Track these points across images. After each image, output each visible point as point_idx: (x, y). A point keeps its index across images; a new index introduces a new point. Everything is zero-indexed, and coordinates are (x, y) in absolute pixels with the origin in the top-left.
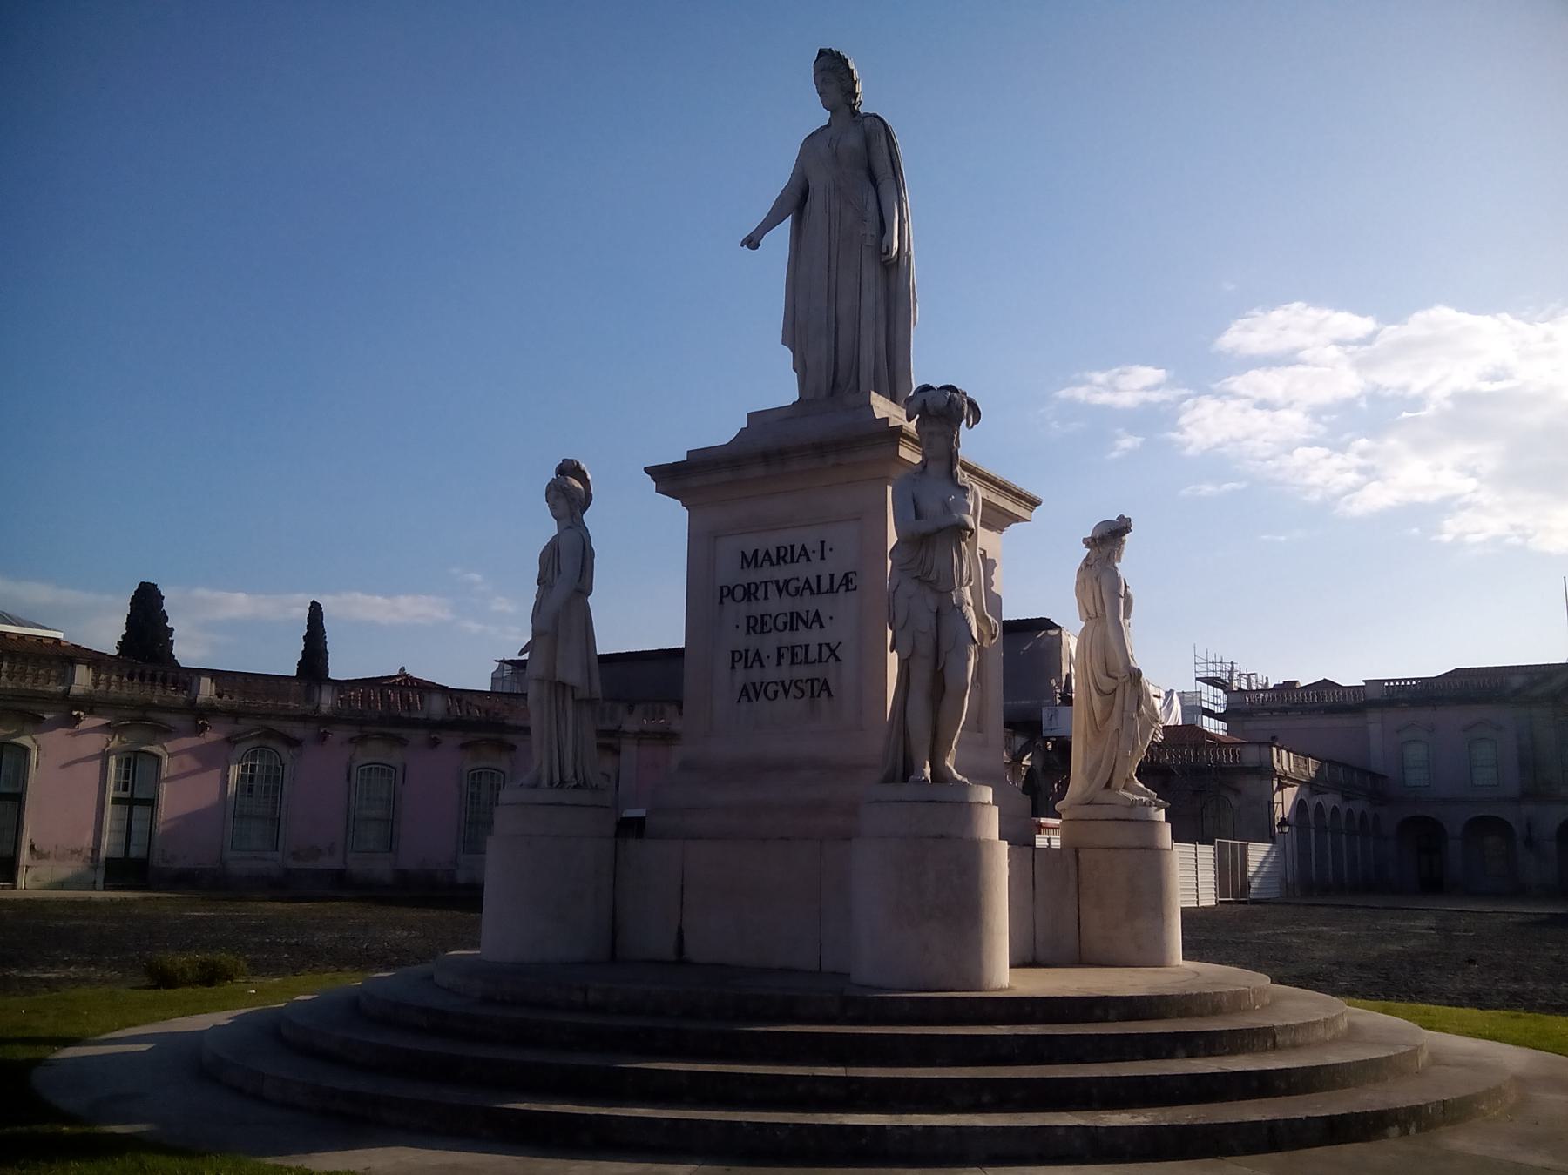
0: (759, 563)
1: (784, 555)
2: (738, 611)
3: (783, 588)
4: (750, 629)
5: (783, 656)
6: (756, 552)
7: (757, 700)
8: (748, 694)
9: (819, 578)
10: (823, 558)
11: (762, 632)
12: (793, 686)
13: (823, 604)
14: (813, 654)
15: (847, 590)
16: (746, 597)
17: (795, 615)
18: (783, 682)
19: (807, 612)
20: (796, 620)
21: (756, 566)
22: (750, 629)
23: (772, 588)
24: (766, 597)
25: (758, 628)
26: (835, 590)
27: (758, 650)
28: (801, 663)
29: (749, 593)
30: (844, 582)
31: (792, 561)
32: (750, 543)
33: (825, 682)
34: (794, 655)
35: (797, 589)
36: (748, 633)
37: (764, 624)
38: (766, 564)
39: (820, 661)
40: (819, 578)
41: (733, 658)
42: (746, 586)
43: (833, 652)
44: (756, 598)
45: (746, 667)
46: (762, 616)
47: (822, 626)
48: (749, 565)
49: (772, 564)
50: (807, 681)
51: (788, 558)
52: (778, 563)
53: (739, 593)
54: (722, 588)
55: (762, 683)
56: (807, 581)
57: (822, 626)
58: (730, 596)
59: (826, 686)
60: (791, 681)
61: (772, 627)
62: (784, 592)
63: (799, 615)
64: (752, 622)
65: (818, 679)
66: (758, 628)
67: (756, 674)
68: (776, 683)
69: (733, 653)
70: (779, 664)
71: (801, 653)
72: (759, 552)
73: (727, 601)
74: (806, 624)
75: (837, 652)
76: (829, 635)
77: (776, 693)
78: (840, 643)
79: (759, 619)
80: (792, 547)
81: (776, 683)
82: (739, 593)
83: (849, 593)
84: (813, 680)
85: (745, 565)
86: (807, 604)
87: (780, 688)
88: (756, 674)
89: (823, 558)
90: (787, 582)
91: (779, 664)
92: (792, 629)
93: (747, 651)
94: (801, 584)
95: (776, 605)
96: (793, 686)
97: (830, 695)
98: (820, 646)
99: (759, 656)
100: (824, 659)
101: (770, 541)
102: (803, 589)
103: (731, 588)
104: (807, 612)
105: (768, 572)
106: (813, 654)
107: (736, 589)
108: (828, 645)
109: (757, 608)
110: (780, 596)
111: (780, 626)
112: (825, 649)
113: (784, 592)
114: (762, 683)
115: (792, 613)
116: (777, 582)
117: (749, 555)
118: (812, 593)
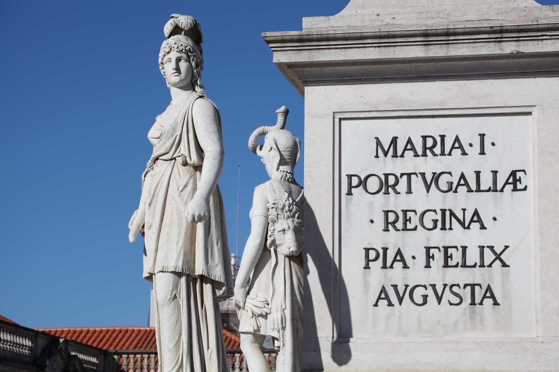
0: (399, 153)
4: (388, 225)
5: (433, 257)
6: (394, 141)
7: (400, 304)
8: (387, 298)
9: (478, 173)
11: (405, 229)
14: (473, 257)
15: (515, 189)
17: (448, 213)
18: (433, 286)
19: (464, 210)
21: (395, 156)
23: (417, 182)
24: (409, 192)
25: (399, 225)
26: (499, 188)
27: (399, 249)
28: (456, 266)
30: (511, 180)
31: (443, 154)
33: (489, 289)
34: (447, 257)
37: (407, 220)
38: (409, 154)
39: (482, 266)
40: (478, 173)
41: (367, 255)
42: (383, 178)
43: (498, 257)
45: (384, 267)
46: (405, 212)
47: (483, 227)
48: (386, 154)
49: (416, 155)
50: (465, 286)
51: (437, 150)
52: (424, 155)
53: (373, 185)
55: (407, 286)
56: (462, 176)
57: (483, 227)
59: (489, 293)
60: (445, 285)
63: (452, 214)
65: (479, 285)
66: (399, 225)
68: (425, 287)
69: (367, 250)
70: (428, 266)
71: (457, 257)
73: (358, 192)
74: (462, 224)
75: (502, 257)
77: (425, 297)
78: (507, 247)
79: (401, 214)
80: (443, 137)
81: (425, 287)
82: (373, 185)
84: (473, 286)
85: (381, 153)
87: (430, 292)
89: (482, 153)
90: (436, 177)
91: (428, 266)
92: (443, 228)
93: (385, 250)
94: (455, 180)
96: (447, 288)
97: (496, 303)
98: (482, 248)
99: (402, 256)
100: (487, 263)
102: (459, 184)
104: (464, 210)
106: (473, 257)
107: (369, 181)
110: (428, 191)
112: (487, 251)
114: (407, 286)
115: (443, 211)
116: (423, 175)
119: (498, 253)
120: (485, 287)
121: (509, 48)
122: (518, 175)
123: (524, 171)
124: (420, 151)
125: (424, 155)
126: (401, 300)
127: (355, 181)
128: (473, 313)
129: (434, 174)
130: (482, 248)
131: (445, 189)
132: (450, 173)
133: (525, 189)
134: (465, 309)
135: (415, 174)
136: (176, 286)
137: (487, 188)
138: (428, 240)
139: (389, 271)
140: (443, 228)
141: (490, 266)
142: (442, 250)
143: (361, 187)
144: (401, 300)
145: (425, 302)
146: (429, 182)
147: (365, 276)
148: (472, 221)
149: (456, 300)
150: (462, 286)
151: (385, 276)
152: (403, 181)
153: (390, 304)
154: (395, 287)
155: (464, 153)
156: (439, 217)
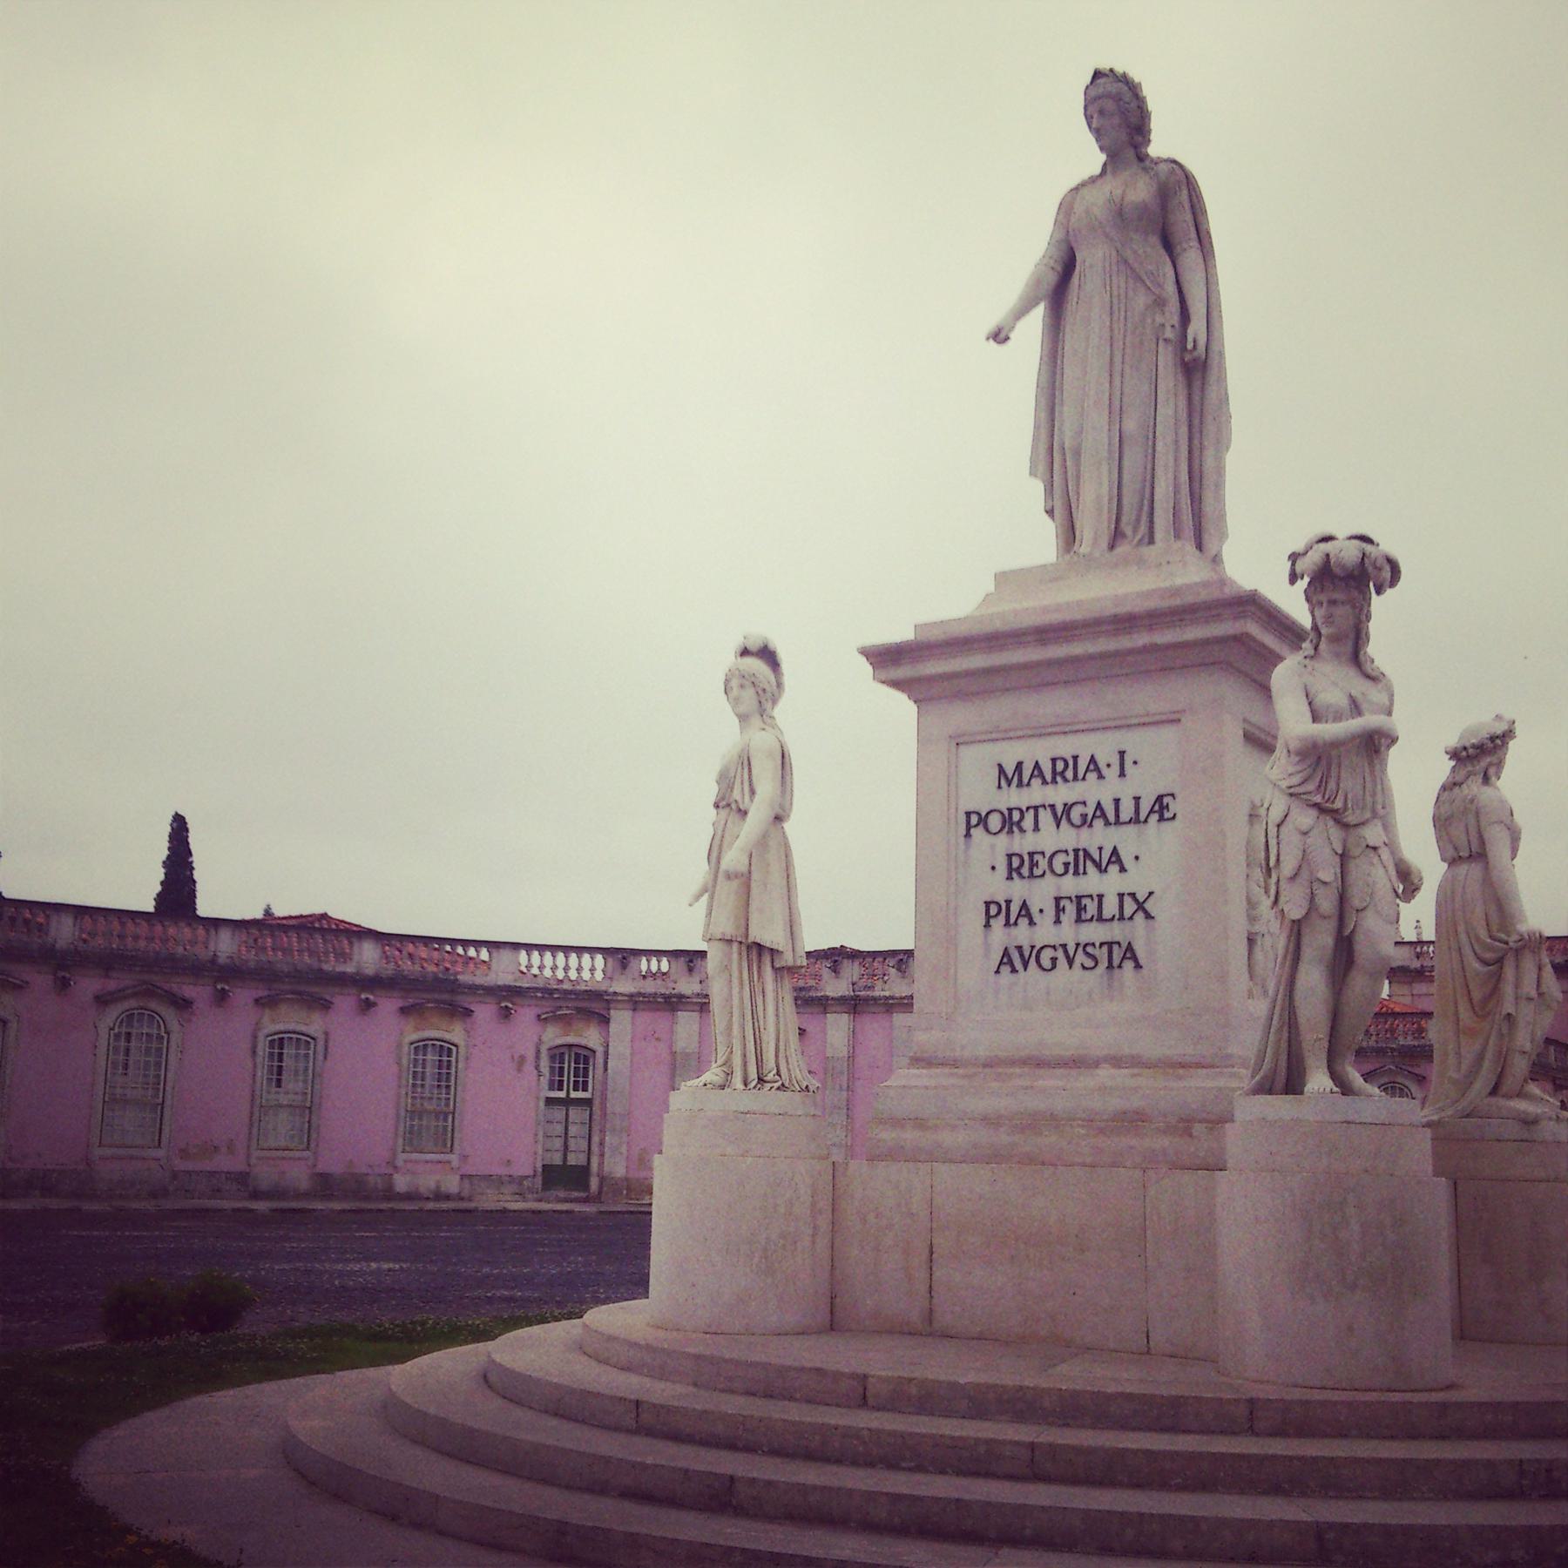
0: (1025, 780)
1: (1063, 770)
2: (991, 848)
3: (1062, 815)
4: (1012, 872)
6: (1019, 765)
7: (1025, 970)
9: (1117, 801)
10: (1122, 774)
11: (1032, 876)
12: (1080, 949)
13: (1125, 839)
14: (1110, 908)
15: (1161, 819)
16: (1006, 829)
17: (1081, 853)
18: (1064, 946)
19: (1100, 849)
20: (1080, 860)
21: (1020, 784)
22: (1012, 872)
23: (1046, 817)
24: (1036, 828)
25: (1025, 871)
26: (1142, 818)
29: (1011, 822)
30: (1156, 808)
32: (1010, 754)
33: (1130, 948)
34: (1081, 909)
35: (1084, 816)
36: (1010, 878)
37: (1033, 865)
38: (1036, 782)
39: (1122, 918)
40: (1117, 801)
41: (987, 911)
42: (1006, 813)
43: (1140, 906)
44: (1022, 831)
45: (1007, 924)
46: (1031, 854)
47: (1123, 869)
48: (1009, 784)
50: (1102, 944)
51: (1069, 774)
52: (1054, 781)
54: (968, 814)
55: (1033, 947)
57: (1123, 869)
58: (981, 826)
59: (1130, 953)
60: (1078, 945)
61: (1046, 867)
62: (1064, 822)
63: (1087, 854)
64: (1016, 862)
65: (1119, 943)
66: (1025, 871)
67: (1022, 934)
69: (988, 904)
70: (1058, 921)
72: (1025, 766)
73: (978, 833)
74: (1098, 865)
75: (1147, 906)
76: (1136, 880)
77: (1054, 960)
78: (1151, 893)
79: (1026, 858)
80: (1075, 758)
81: (1054, 947)
82: (995, 822)
83: (1165, 825)
84: (1110, 944)
85: (1003, 783)
86: (1098, 838)
87: (1060, 954)
88: (1022, 934)
89: (1122, 774)
90: (1068, 808)
91: (1058, 921)
92: (1076, 873)
93: (1008, 902)
94: (1090, 811)
95: (1050, 838)
96: (1080, 949)
97: (1138, 966)
98: (1121, 896)
99: (1028, 910)
101: (1040, 752)
102: (1094, 816)
103: (983, 814)
104: (1100, 849)
105: (1037, 793)
106: (1110, 908)
108: (1133, 895)
109: (1024, 843)
110: (1058, 826)
111: (1059, 869)
112: (1128, 901)
113: (1064, 822)
114: (1033, 947)
115: (1076, 851)
116: (1052, 807)
117: (1010, 770)
118: (1107, 823)
119: (1141, 900)
120: (1124, 945)
121: (1141, 639)
122: (1165, 800)
123: (1172, 795)
124: (1049, 777)
125: (1054, 781)
126: (1025, 965)
127: (974, 820)
128: (1111, 978)
129: (1065, 805)
130: (1121, 896)
131: (1079, 823)
132: (1084, 803)
133: (1174, 817)
134: (1102, 976)
135: (1044, 806)
136: (729, 956)
137: (1128, 820)
138: (1059, 888)
139: (1014, 931)
140: (1076, 873)
141: (1131, 918)
142: (1074, 899)
143: (981, 826)
144: (1025, 965)
145: (1054, 967)
146: (1059, 815)
147: (986, 937)
148: (1109, 862)
149: (1089, 963)
150: (1097, 945)
151: (1009, 935)
152: (1030, 816)
153: (1014, 970)
154: (1019, 948)
155: (1101, 777)
156: (1071, 859)
